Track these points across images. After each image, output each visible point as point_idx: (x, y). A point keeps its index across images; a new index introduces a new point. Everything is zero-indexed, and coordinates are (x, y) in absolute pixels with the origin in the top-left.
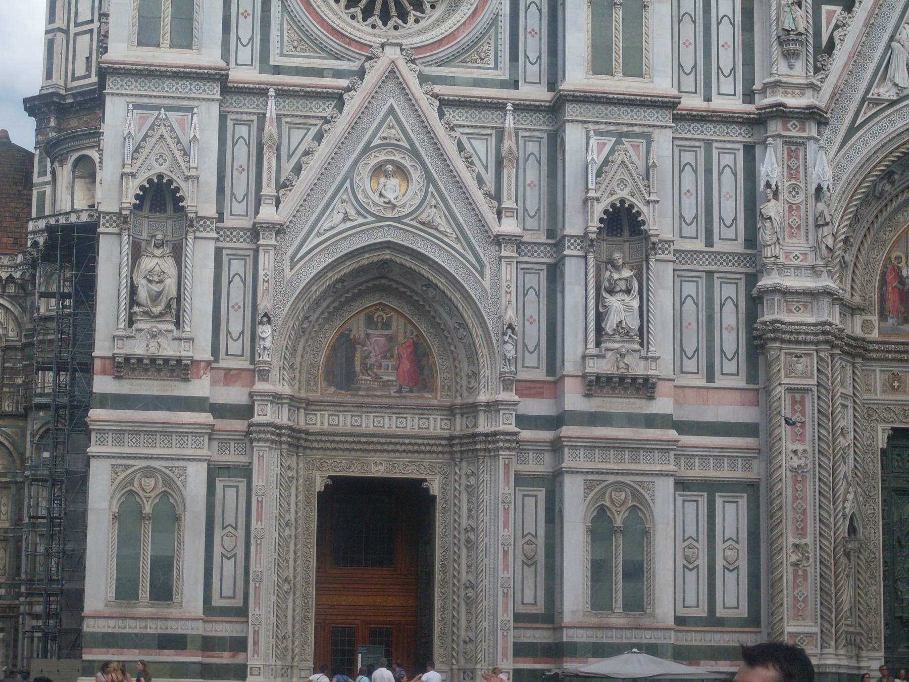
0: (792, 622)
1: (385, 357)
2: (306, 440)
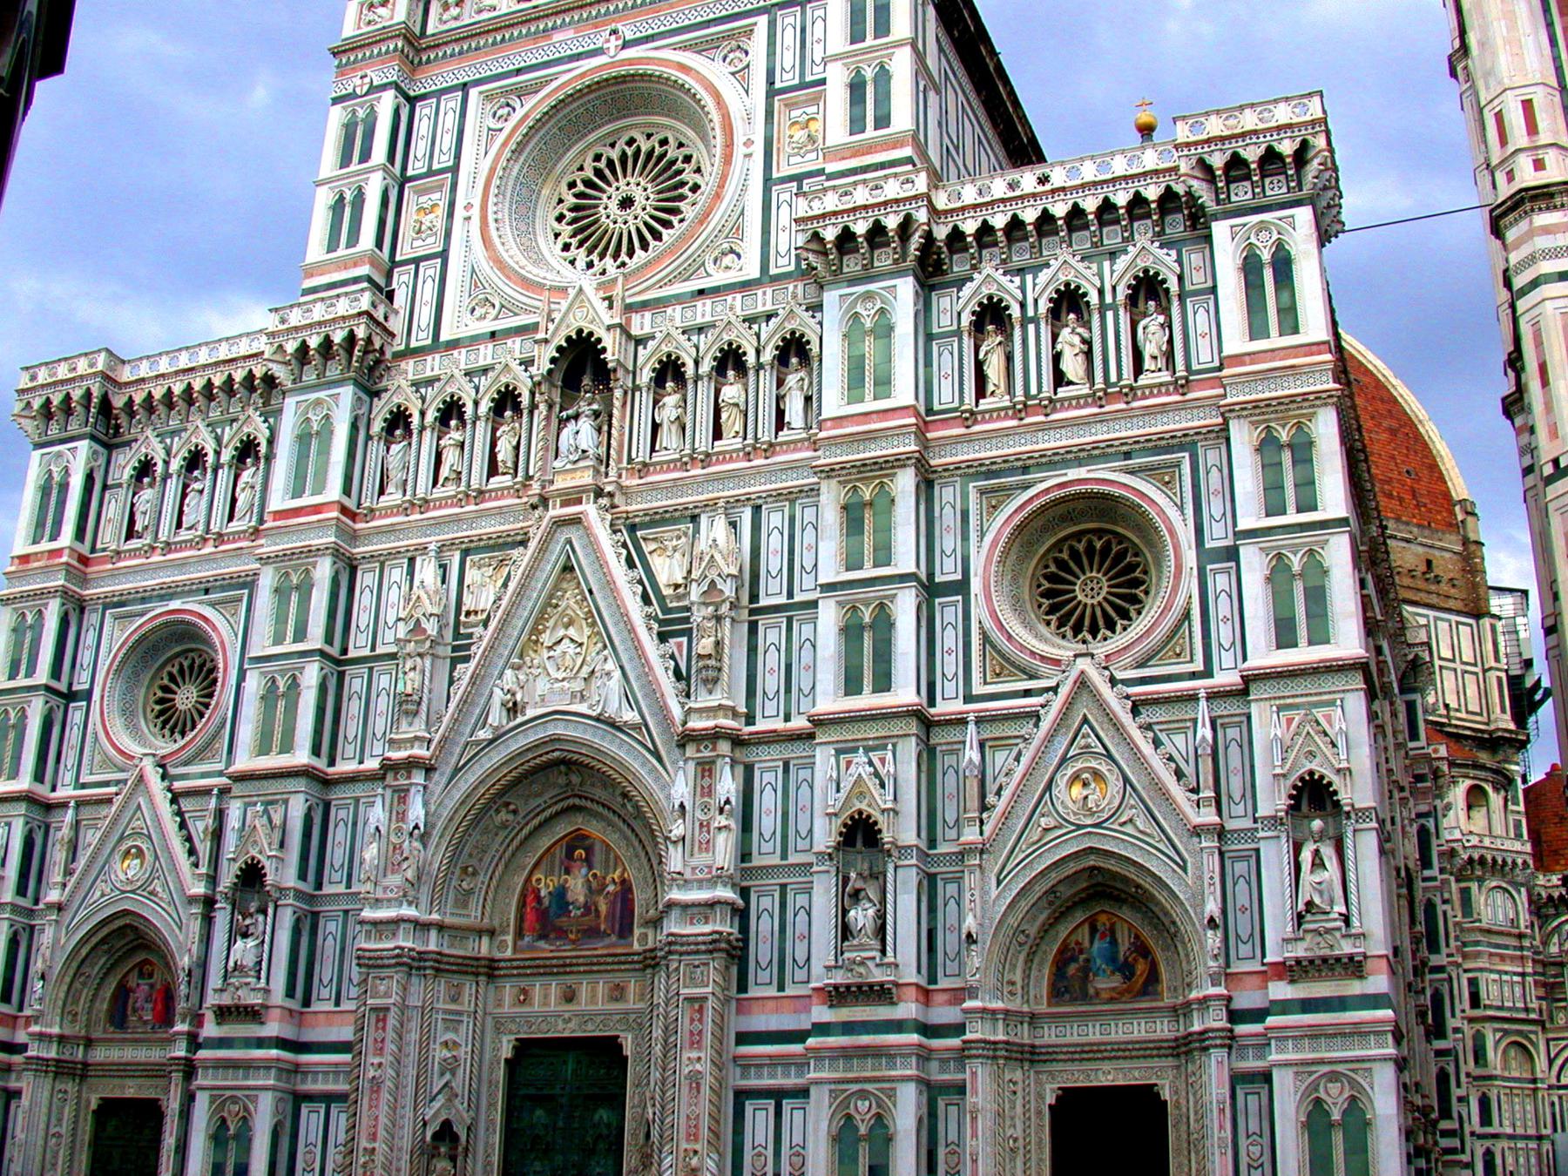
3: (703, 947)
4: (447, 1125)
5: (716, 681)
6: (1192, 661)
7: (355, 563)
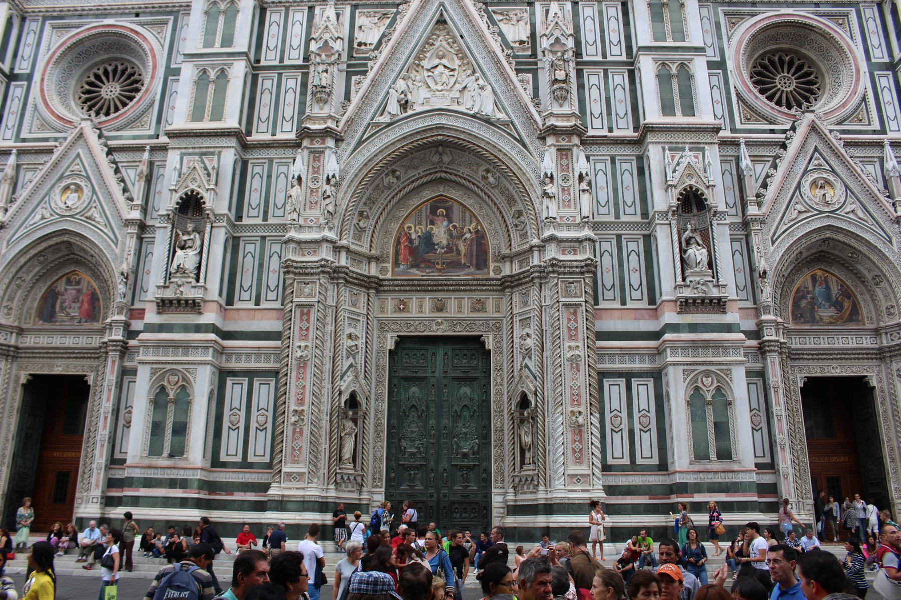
0: (289, 465)
1: (74, 302)
2: (18, 353)
3: (577, 270)
4: (353, 396)
5: (565, 99)
6: (870, 125)
7: (265, 6)
